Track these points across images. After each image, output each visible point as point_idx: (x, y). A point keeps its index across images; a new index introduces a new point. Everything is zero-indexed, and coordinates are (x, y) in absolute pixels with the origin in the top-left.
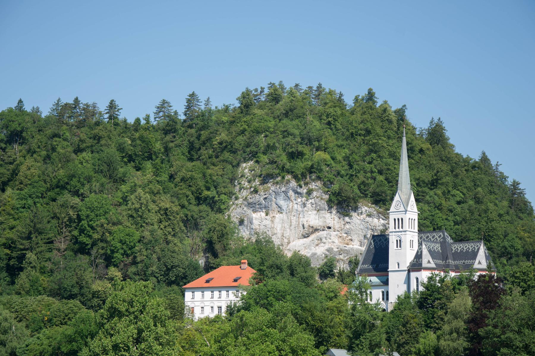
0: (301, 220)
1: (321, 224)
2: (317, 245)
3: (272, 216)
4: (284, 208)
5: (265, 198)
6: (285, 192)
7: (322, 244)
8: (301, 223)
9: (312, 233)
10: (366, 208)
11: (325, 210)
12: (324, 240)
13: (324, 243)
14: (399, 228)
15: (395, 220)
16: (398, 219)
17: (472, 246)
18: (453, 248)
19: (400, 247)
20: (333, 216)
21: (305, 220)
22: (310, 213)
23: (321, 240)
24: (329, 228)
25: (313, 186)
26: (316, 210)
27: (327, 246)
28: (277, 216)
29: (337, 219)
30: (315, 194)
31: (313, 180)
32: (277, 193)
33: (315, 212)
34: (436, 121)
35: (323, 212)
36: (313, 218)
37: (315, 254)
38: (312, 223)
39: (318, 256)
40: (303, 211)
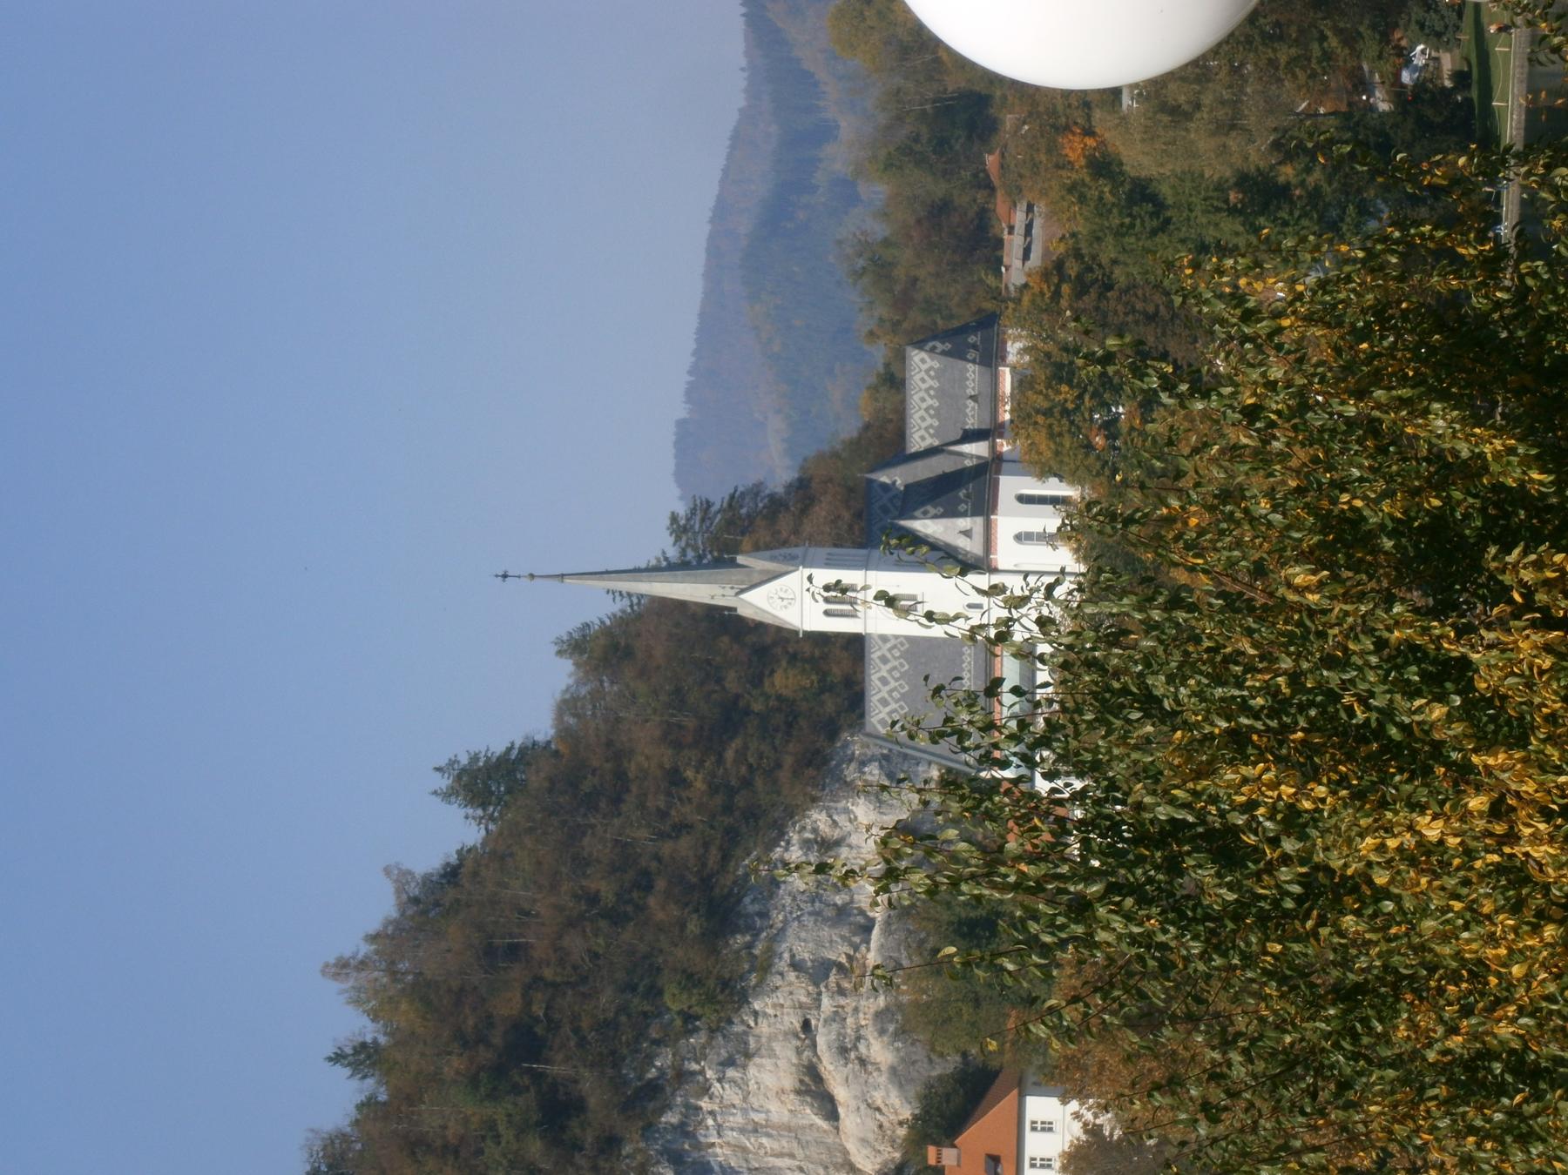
10: (747, 900)
11: (745, 1033)
15: (827, 613)
17: (923, 380)
18: (924, 445)
20: (770, 1011)
22: (752, 1086)
24: (806, 1025)
26: (744, 1067)
27: (870, 1033)
33: (752, 1071)
35: (752, 1041)
36: (770, 1079)
37: (893, 1070)
39: (903, 1060)
40: (744, 1111)
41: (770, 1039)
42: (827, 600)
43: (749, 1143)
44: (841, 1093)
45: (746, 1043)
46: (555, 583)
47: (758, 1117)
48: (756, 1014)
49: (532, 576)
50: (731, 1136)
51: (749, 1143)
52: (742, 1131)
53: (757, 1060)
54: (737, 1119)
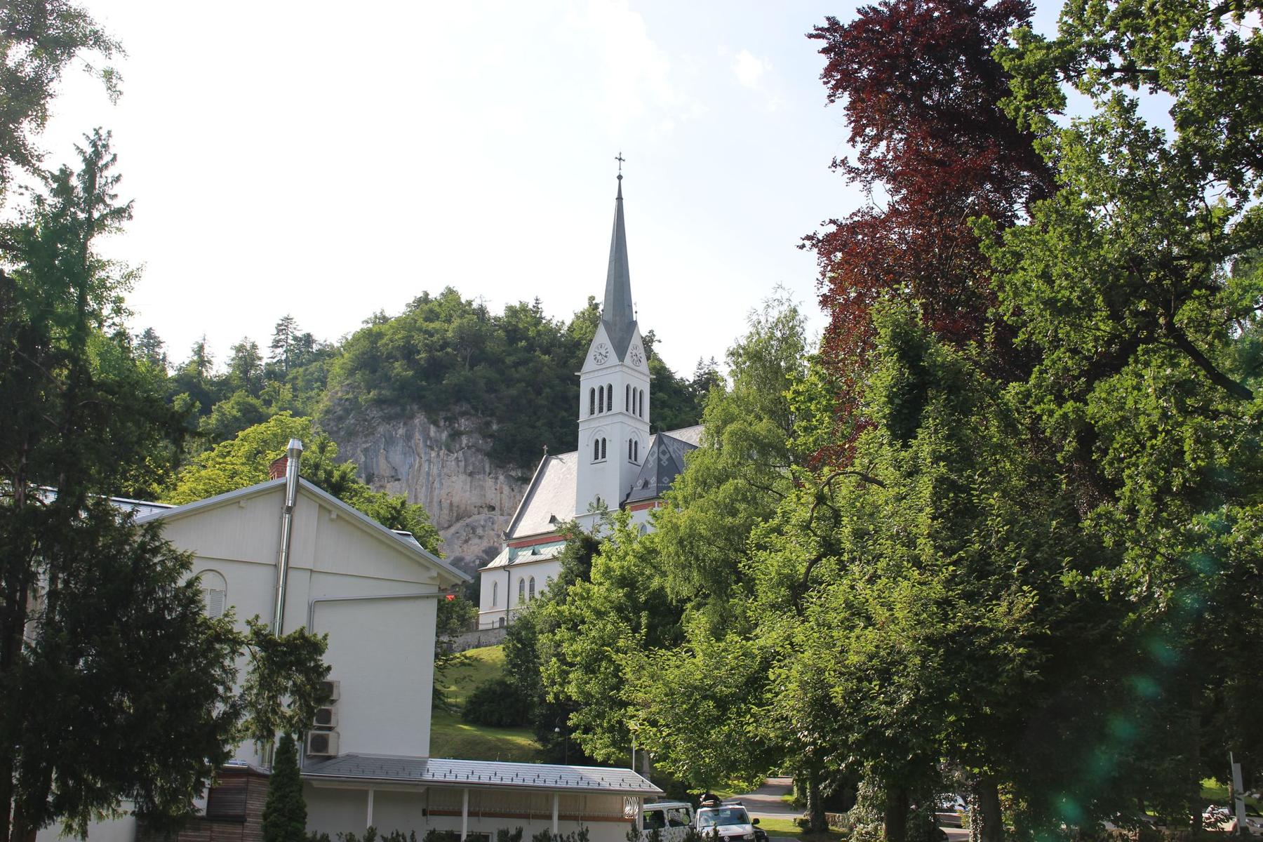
0: (437, 492)
1: (474, 500)
2: (466, 541)
3: (378, 484)
4: (403, 470)
5: (366, 451)
6: (409, 437)
7: (476, 541)
8: (435, 499)
9: (459, 519)
12: (480, 531)
13: (480, 537)
14: (601, 410)
15: (593, 391)
16: (602, 389)
19: (604, 456)
21: (444, 492)
22: (454, 478)
23: (474, 529)
24: (493, 508)
25: (463, 424)
26: (465, 472)
28: (388, 485)
29: (506, 489)
30: (464, 440)
31: (463, 414)
32: (390, 441)
33: (462, 477)
34: (707, 361)
35: (481, 476)
38: (456, 500)
40: (439, 475)
41: (482, 488)
42: (602, 389)
43: (422, 480)
44: (452, 530)
45: (479, 473)
46: (616, 195)
47: (437, 485)
48: (497, 478)
49: (620, 177)
50: (425, 467)
51: (422, 480)
52: (428, 474)
53: (469, 479)
54: (435, 471)
